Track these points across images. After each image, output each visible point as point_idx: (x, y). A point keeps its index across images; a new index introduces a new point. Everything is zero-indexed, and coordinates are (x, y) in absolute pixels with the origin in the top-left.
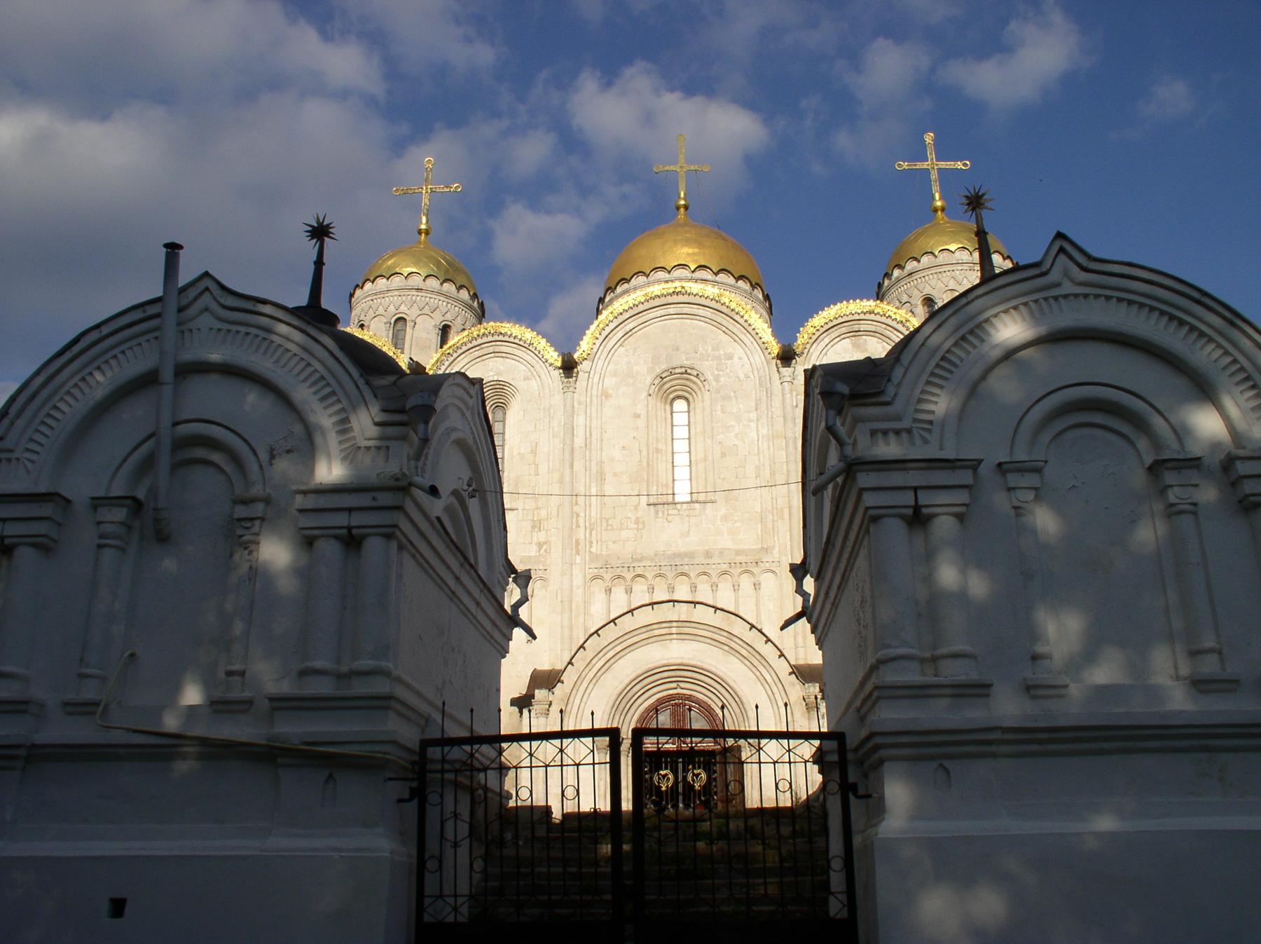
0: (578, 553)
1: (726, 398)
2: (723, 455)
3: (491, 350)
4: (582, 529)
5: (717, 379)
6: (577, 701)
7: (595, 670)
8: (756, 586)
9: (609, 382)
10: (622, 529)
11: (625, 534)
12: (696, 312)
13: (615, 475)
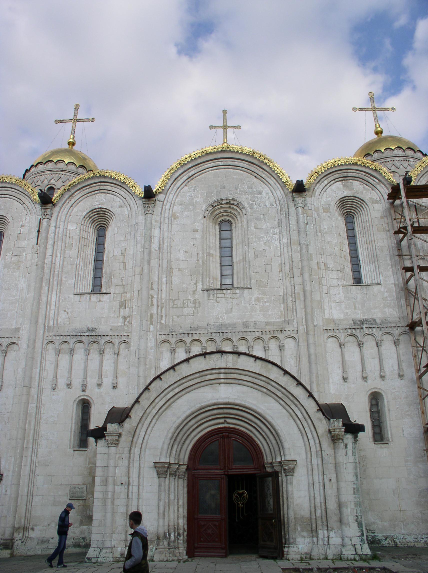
0: (151, 323)
1: (258, 219)
2: (256, 256)
3: (97, 188)
4: (155, 307)
5: (251, 207)
6: (143, 434)
7: (157, 408)
9: (176, 208)
10: (183, 307)
11: (186, 311)
12: (236, 164)
13: (180, 270)
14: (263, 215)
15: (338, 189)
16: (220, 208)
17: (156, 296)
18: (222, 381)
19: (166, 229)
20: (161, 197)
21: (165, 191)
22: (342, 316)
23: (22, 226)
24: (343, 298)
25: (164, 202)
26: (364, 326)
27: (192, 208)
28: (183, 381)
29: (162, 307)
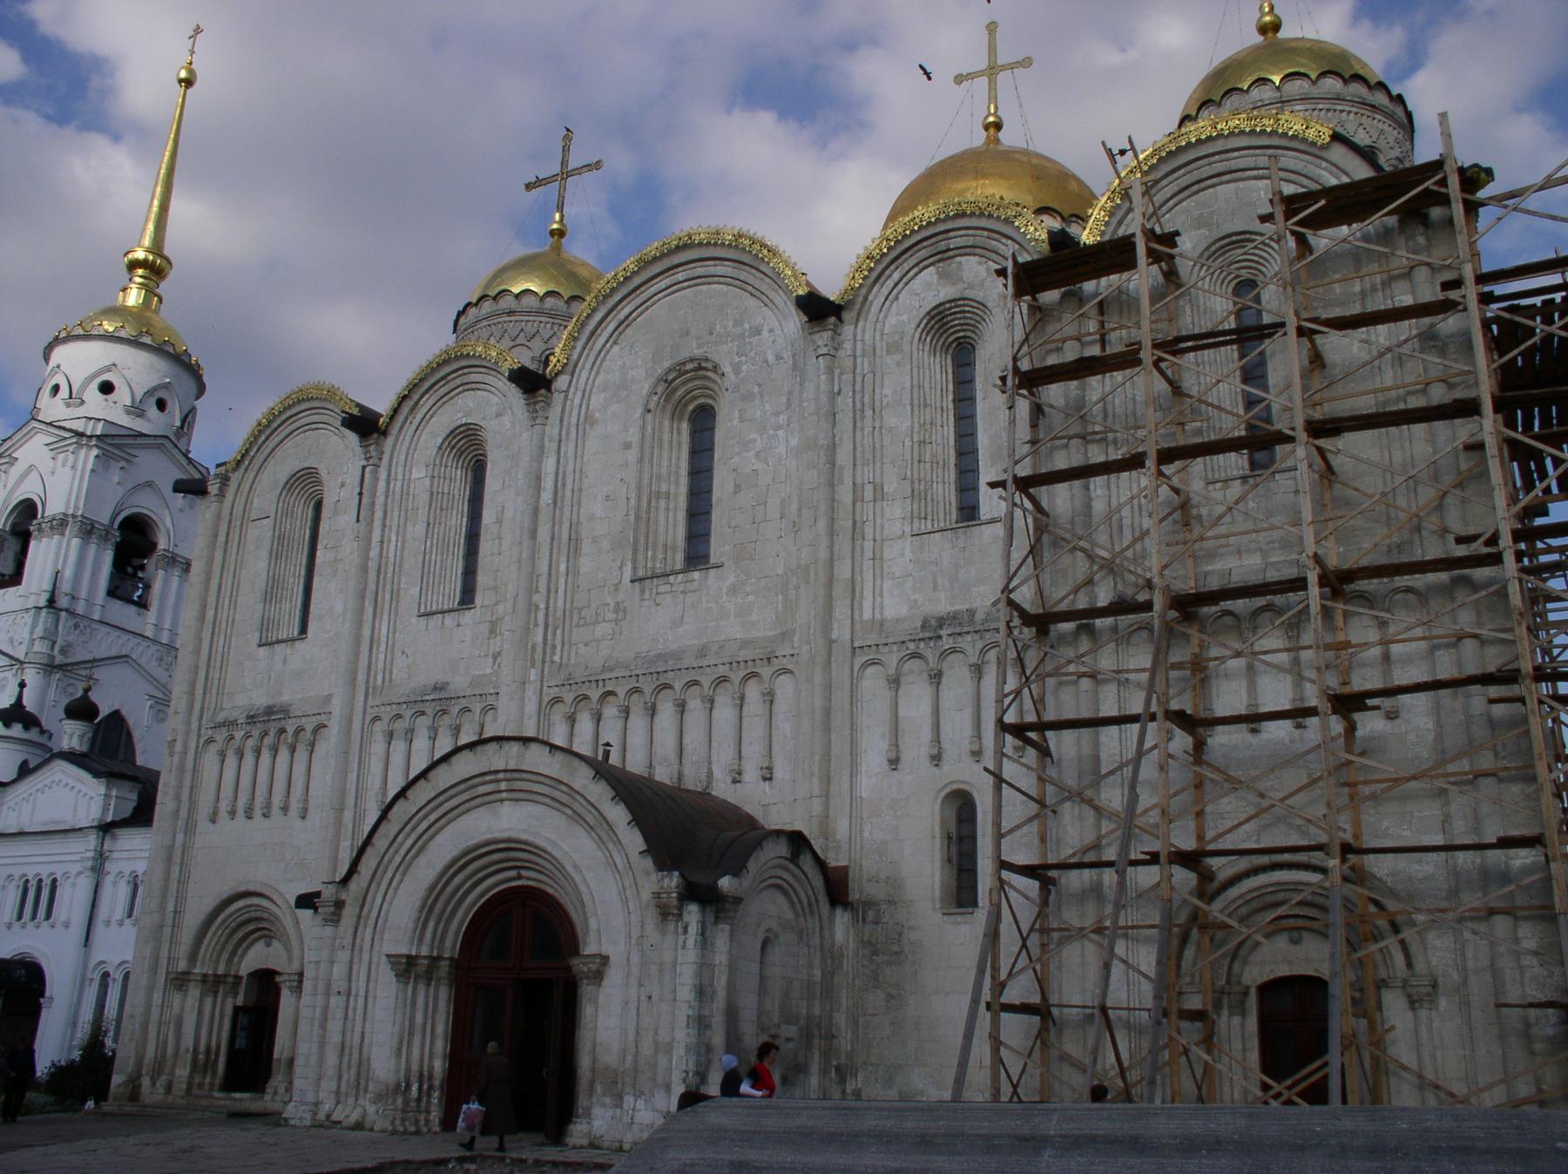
1: (748, 397)
2: (738, 488)
5: (737, 371)
6: (379, 901)
7: (403, 851)
8: (770, 697)
10: (597, 623)
11: (602, 630)
12: (712, 270)
13: (594, 540)
14: (760, 385)
15: (928, 286)
16: (685, 383)
17: (542, 606)
18: (504, 795)
19: (571, 453)
20: (561, 382)
21: (570, 368)
22: (904, 611)
23: (343, 485)
24: (910, 567)
25: (567, 391)
26: (944, 632)
27: (624, 394)
28: (441, 798)
29: (556, 628)
